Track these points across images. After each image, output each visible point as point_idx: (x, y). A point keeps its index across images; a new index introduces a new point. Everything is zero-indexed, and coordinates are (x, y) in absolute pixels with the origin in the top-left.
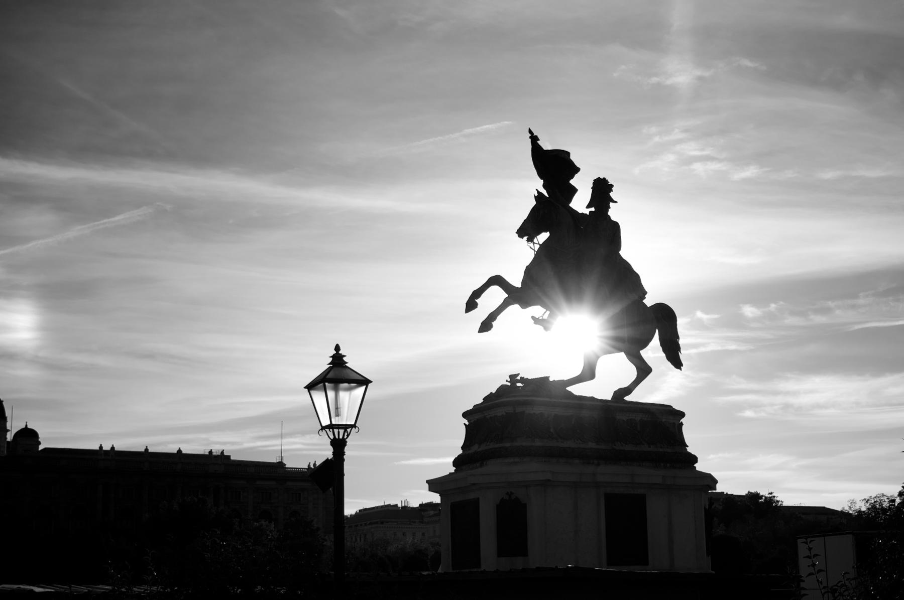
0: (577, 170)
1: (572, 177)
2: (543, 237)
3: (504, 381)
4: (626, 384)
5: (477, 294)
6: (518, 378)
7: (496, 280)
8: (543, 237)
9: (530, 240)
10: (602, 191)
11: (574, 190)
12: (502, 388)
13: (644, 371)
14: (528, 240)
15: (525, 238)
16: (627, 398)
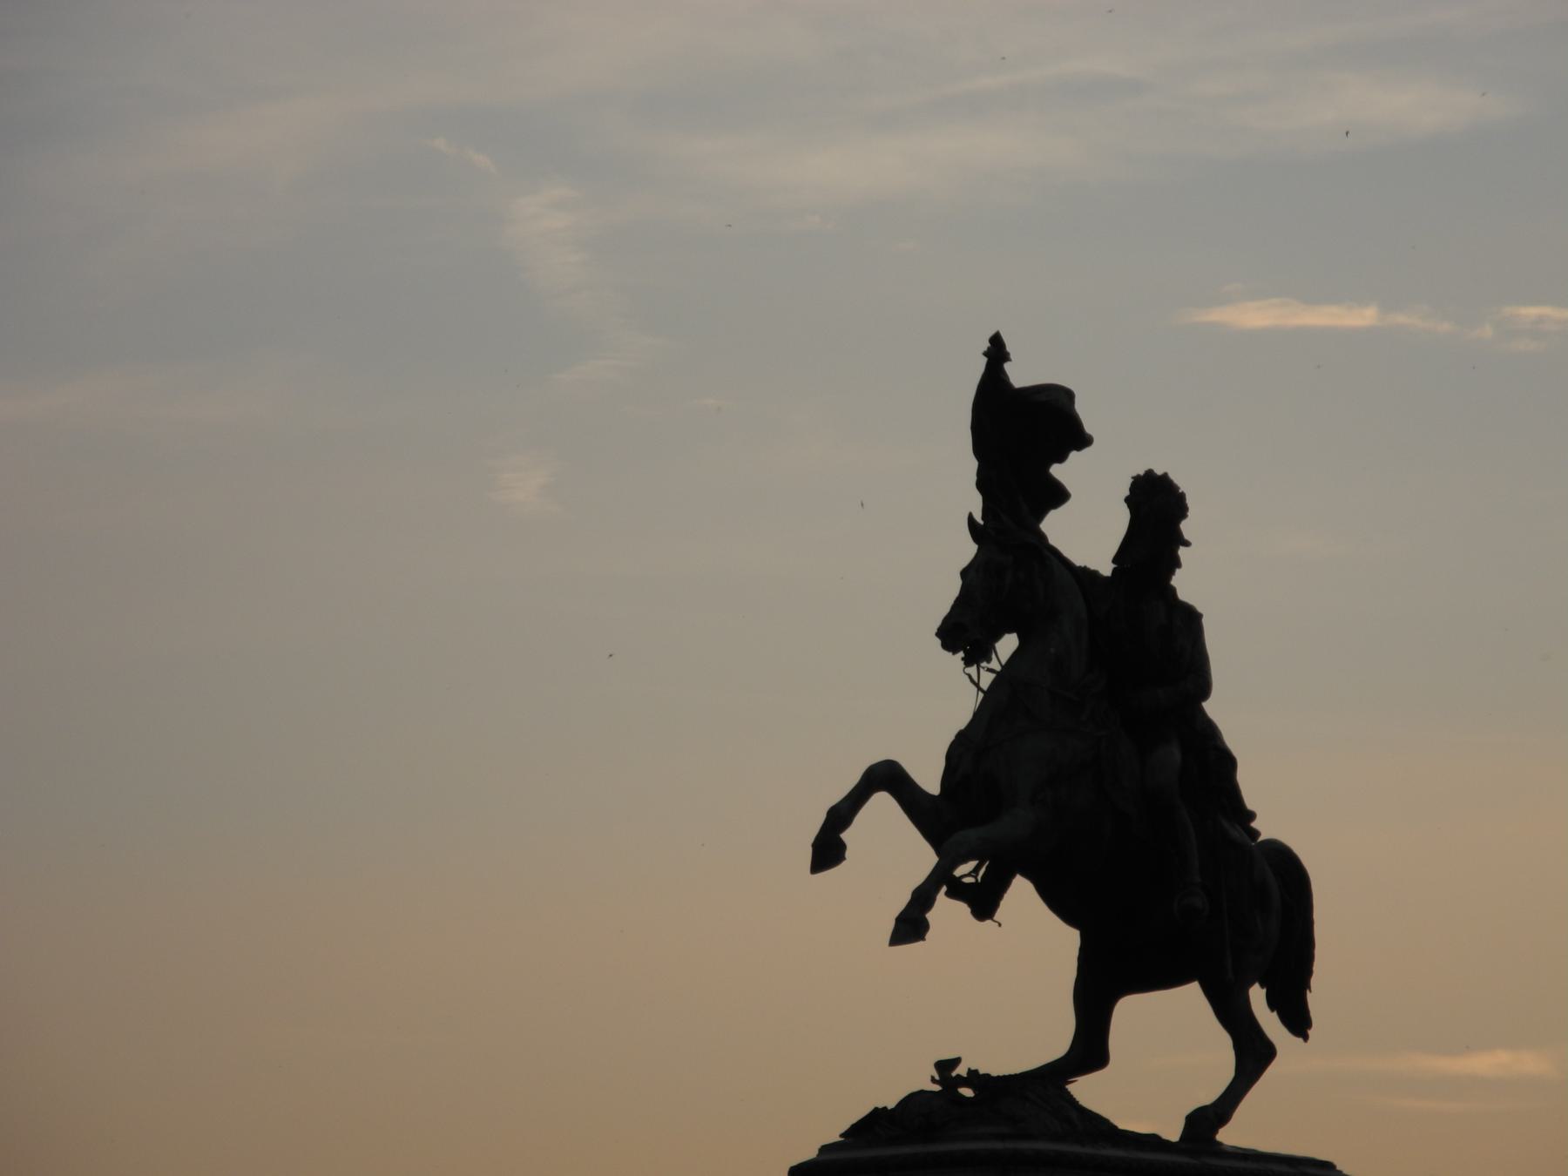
0: (1083, 441)
1: (1061, 458)
2: (1007, 645)
3: (923, 1080)
4: (1208, 1094)
5: (841, 816)
6: (961, 1070)
7: (887, 777)
8: (1007, 645)
9: (976, 654)
10: (1156, 508)
11: (1058, 495)
12: (914, 1101)
13: (1253, 1055)
14: (968, 662)
15: (961, 654)
16: (1228, 1136)
